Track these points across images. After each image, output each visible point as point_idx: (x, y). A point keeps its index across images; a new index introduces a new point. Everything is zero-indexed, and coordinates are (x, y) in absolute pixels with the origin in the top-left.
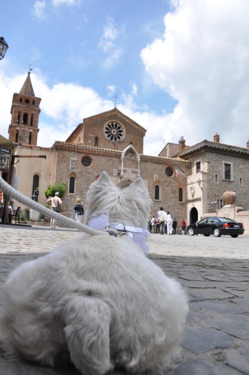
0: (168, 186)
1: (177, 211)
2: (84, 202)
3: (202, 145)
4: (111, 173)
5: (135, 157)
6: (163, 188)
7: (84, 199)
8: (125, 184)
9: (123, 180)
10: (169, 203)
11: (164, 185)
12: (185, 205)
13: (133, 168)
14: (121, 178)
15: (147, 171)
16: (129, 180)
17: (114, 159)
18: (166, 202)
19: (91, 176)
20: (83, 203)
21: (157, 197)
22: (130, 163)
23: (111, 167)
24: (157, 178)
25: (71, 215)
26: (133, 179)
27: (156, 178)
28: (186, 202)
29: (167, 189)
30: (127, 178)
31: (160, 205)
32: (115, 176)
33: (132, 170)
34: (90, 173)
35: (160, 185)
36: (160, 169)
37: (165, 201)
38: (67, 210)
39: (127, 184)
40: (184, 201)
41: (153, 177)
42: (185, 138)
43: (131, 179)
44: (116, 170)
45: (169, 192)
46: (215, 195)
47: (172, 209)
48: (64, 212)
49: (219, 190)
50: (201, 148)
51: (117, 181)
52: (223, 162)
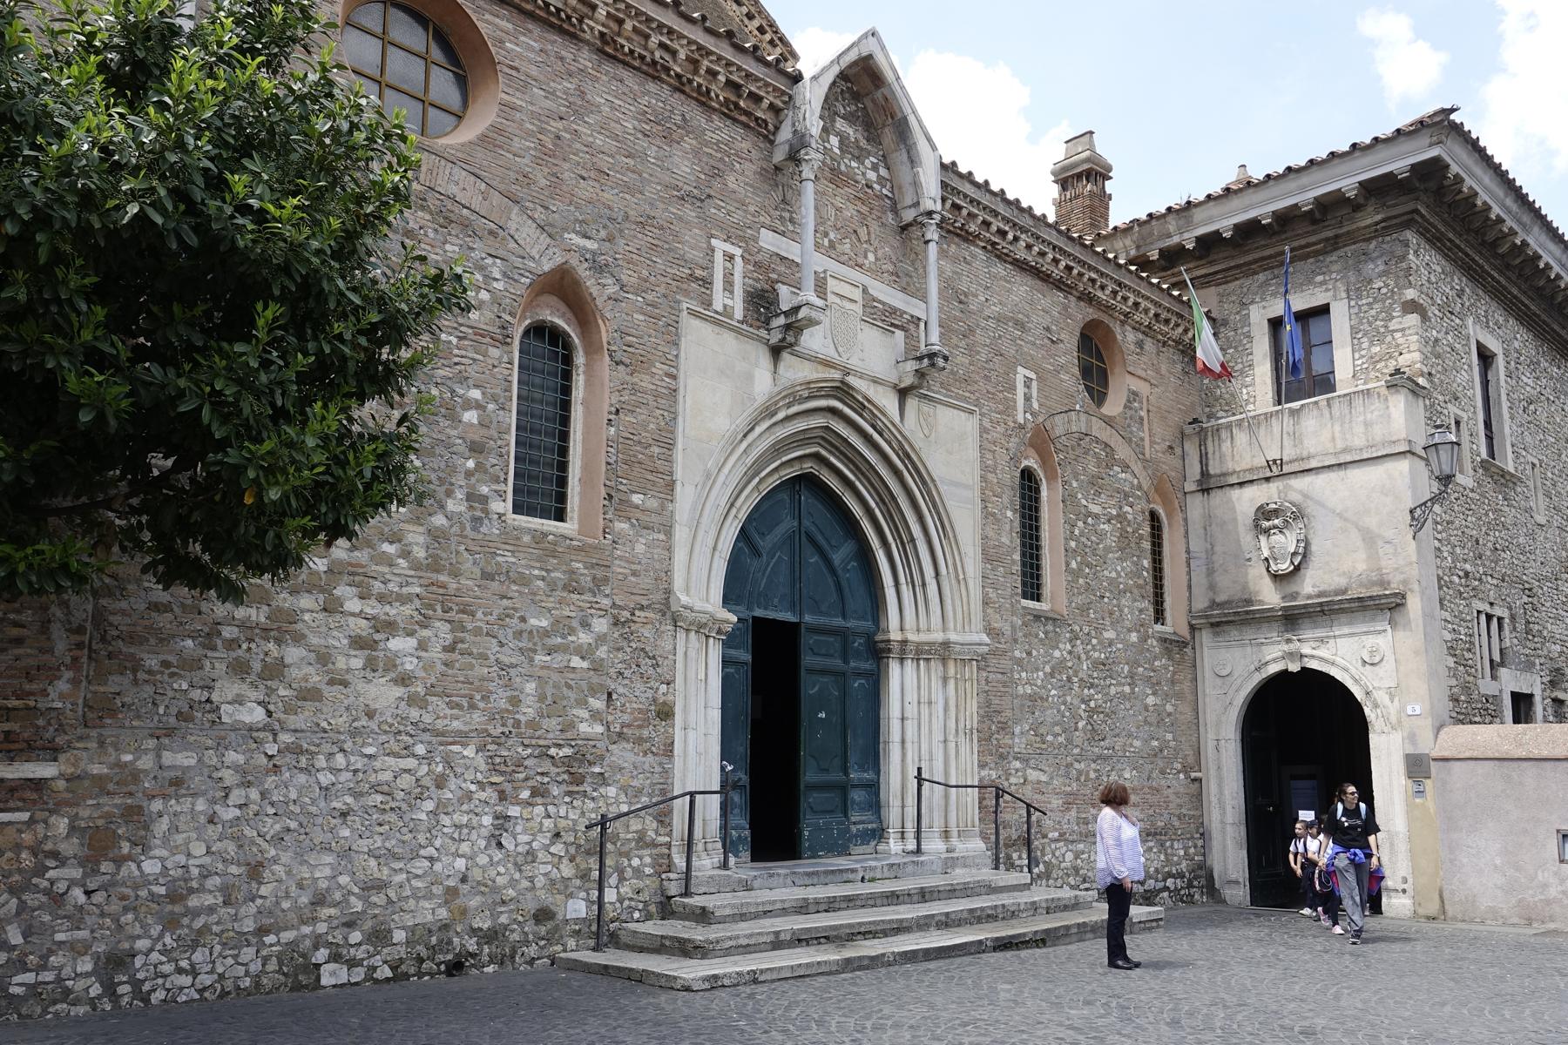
0: (1095, 485)
1: (1151, 700)
2: (381, 599)
3: (1398, 163)
4: (692, 277)
5: (883, 172)
6: (1069, 500)
7: (388, 548)
8: (800, 425)
9: (795, 371)
10: (1110, 634)
11: (1076, 476)
12: (1188, 650)
13: (876, 272)
14: (776, 352)
15: (972, 331)
16: (843, 391)
17: (720, 131)
18: (1089, 623)
19: (482, 268)
20: (373, 608)
21: (1032, 586)
22: (850, 211)
23: (690, 213)
24: (1036, 405)
25: (177, 784)
26: (875, 381)
27: (1028, 398)
28: (1192, 628)
29: (1095, 509)
30: (827, 364)
31: (1057, 654)
32: (727, 311)
33: (865, 290)
34: (465, 225)
35: (1051, 477)
36: (1048, 329)
37: (1084, 609)
38: (100, 712)
39: (818, 421)
40: (1176, 622)
41: (1013, 388)
42: (1105, 149)
43: (862, 376)
44: (738, 252)
45: (1102, 535)
46: (1467, 574)
47: (1127, 689)
48: (52, 752)
49: (1477, 542)
50: (1378, 189)
51: (749, 378)
52: (1476, 332)
